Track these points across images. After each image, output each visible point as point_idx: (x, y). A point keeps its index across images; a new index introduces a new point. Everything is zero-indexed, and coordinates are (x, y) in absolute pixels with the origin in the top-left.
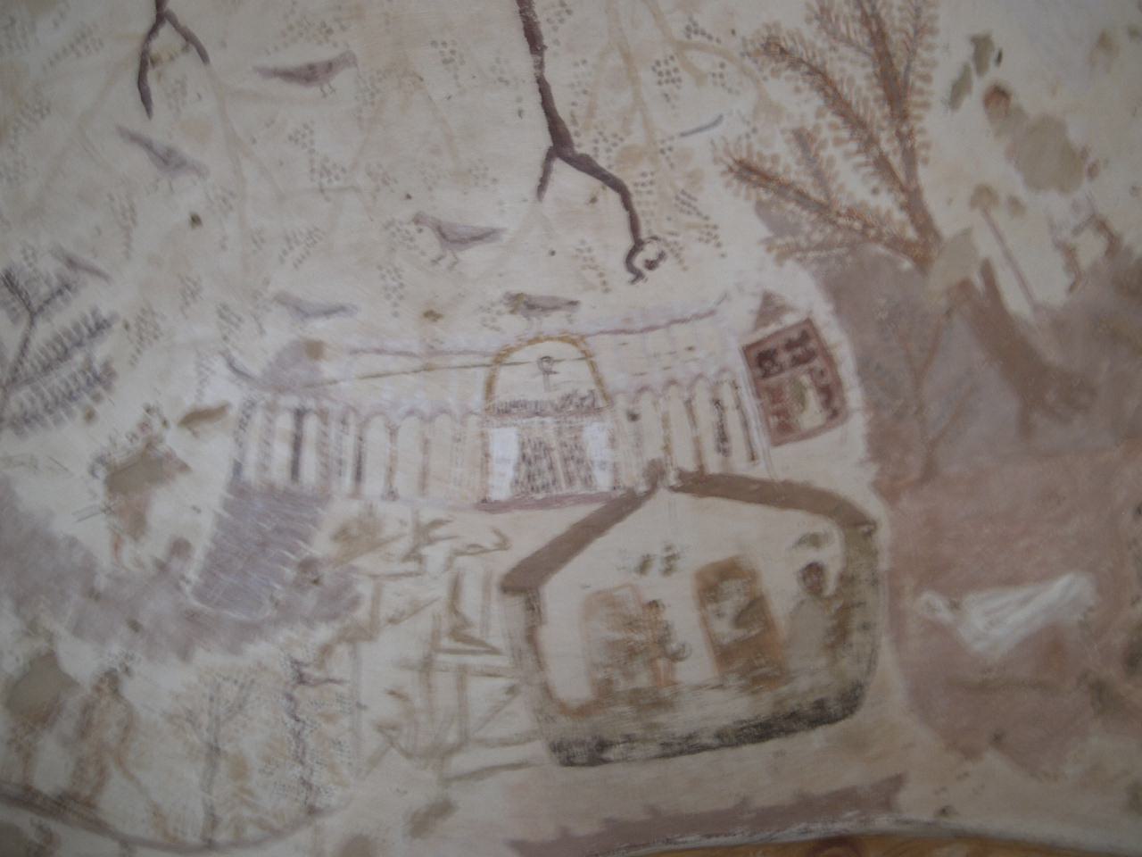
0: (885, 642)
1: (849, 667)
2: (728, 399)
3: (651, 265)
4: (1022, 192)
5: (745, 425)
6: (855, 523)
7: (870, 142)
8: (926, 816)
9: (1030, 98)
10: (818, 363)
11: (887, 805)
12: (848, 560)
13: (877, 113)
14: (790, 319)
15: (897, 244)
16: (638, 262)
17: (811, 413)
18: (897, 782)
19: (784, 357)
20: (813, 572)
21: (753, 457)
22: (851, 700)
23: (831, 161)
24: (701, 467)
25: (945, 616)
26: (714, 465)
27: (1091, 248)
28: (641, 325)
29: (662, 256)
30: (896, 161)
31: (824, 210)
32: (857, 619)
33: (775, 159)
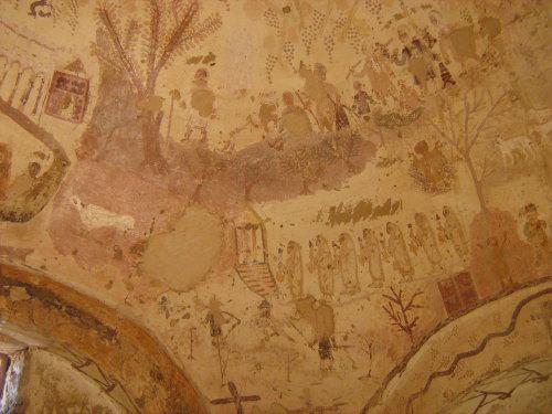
0: (50, 203)
1: (32, 205)
2: (37, 84)
3: (42, 14)
4: (188, 103)
5: (39, 98)
6: (62, 161)
7: (154, 47)
8: (36, 265)
9: (212, 83)
10: (81, 97)
11: (23, 257)
12: (51, 169)
13: (163, 42)
14: (81, 75)
15: (137, 83)
16: (38, 9)
17: (68, 112)
18: (31, 251)
19: (70, 86)
20: (35, 167)
21: (34, 112)
22: (26, 217)
23: (136, 40)
24: (10, 102)
25: (79, 207)
26: (16, 104)
27: (196, 135)
28: (20, 31)
29: (49, 14)
30: (157, 59)
31: (122, 55)
32: (45, 190)
33: (118, 21)
